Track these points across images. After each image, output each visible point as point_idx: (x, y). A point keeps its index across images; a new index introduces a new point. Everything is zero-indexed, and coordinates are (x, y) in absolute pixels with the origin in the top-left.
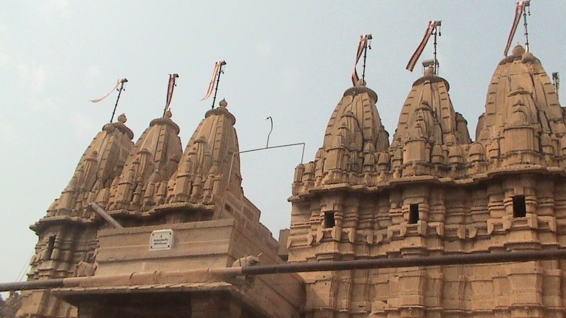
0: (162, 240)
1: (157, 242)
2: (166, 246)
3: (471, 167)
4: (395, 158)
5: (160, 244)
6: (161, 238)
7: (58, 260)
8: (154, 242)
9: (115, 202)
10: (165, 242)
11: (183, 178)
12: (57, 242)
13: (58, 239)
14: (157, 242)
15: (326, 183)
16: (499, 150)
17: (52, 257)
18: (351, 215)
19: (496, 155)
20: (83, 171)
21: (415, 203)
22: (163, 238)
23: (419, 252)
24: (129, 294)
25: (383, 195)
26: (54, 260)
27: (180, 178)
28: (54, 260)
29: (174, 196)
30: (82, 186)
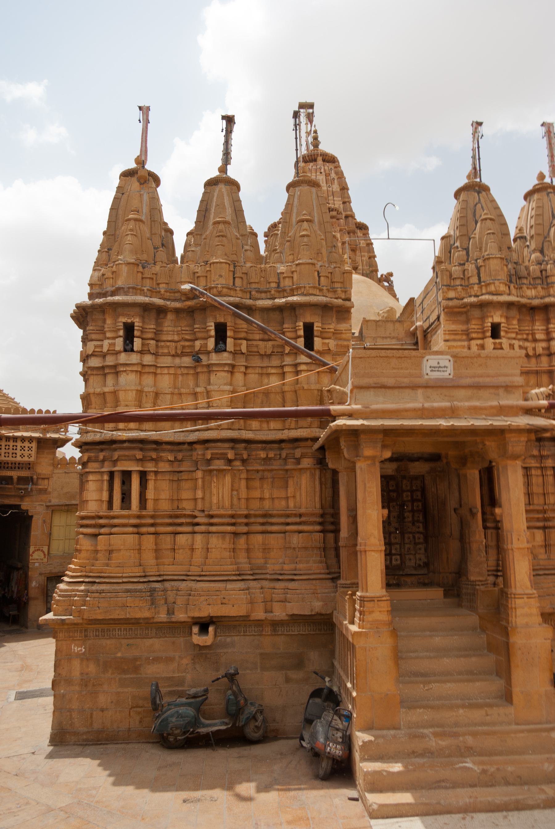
0: (440, 367)
1: (434, 369)
2: (446, 374)
5: (438, 371)
6: (439, 366)
8: (431, 369)
10: (445, 369)
11: (307, 266)
12: (138, 330)
13: (138, 326)
14: (433, 369)
17: (135, 349)
18: (513, 327)
22: (442, 364)
24: (443, 429)
27: (303, 266)
28: (137, 352)
29: (305, 287)
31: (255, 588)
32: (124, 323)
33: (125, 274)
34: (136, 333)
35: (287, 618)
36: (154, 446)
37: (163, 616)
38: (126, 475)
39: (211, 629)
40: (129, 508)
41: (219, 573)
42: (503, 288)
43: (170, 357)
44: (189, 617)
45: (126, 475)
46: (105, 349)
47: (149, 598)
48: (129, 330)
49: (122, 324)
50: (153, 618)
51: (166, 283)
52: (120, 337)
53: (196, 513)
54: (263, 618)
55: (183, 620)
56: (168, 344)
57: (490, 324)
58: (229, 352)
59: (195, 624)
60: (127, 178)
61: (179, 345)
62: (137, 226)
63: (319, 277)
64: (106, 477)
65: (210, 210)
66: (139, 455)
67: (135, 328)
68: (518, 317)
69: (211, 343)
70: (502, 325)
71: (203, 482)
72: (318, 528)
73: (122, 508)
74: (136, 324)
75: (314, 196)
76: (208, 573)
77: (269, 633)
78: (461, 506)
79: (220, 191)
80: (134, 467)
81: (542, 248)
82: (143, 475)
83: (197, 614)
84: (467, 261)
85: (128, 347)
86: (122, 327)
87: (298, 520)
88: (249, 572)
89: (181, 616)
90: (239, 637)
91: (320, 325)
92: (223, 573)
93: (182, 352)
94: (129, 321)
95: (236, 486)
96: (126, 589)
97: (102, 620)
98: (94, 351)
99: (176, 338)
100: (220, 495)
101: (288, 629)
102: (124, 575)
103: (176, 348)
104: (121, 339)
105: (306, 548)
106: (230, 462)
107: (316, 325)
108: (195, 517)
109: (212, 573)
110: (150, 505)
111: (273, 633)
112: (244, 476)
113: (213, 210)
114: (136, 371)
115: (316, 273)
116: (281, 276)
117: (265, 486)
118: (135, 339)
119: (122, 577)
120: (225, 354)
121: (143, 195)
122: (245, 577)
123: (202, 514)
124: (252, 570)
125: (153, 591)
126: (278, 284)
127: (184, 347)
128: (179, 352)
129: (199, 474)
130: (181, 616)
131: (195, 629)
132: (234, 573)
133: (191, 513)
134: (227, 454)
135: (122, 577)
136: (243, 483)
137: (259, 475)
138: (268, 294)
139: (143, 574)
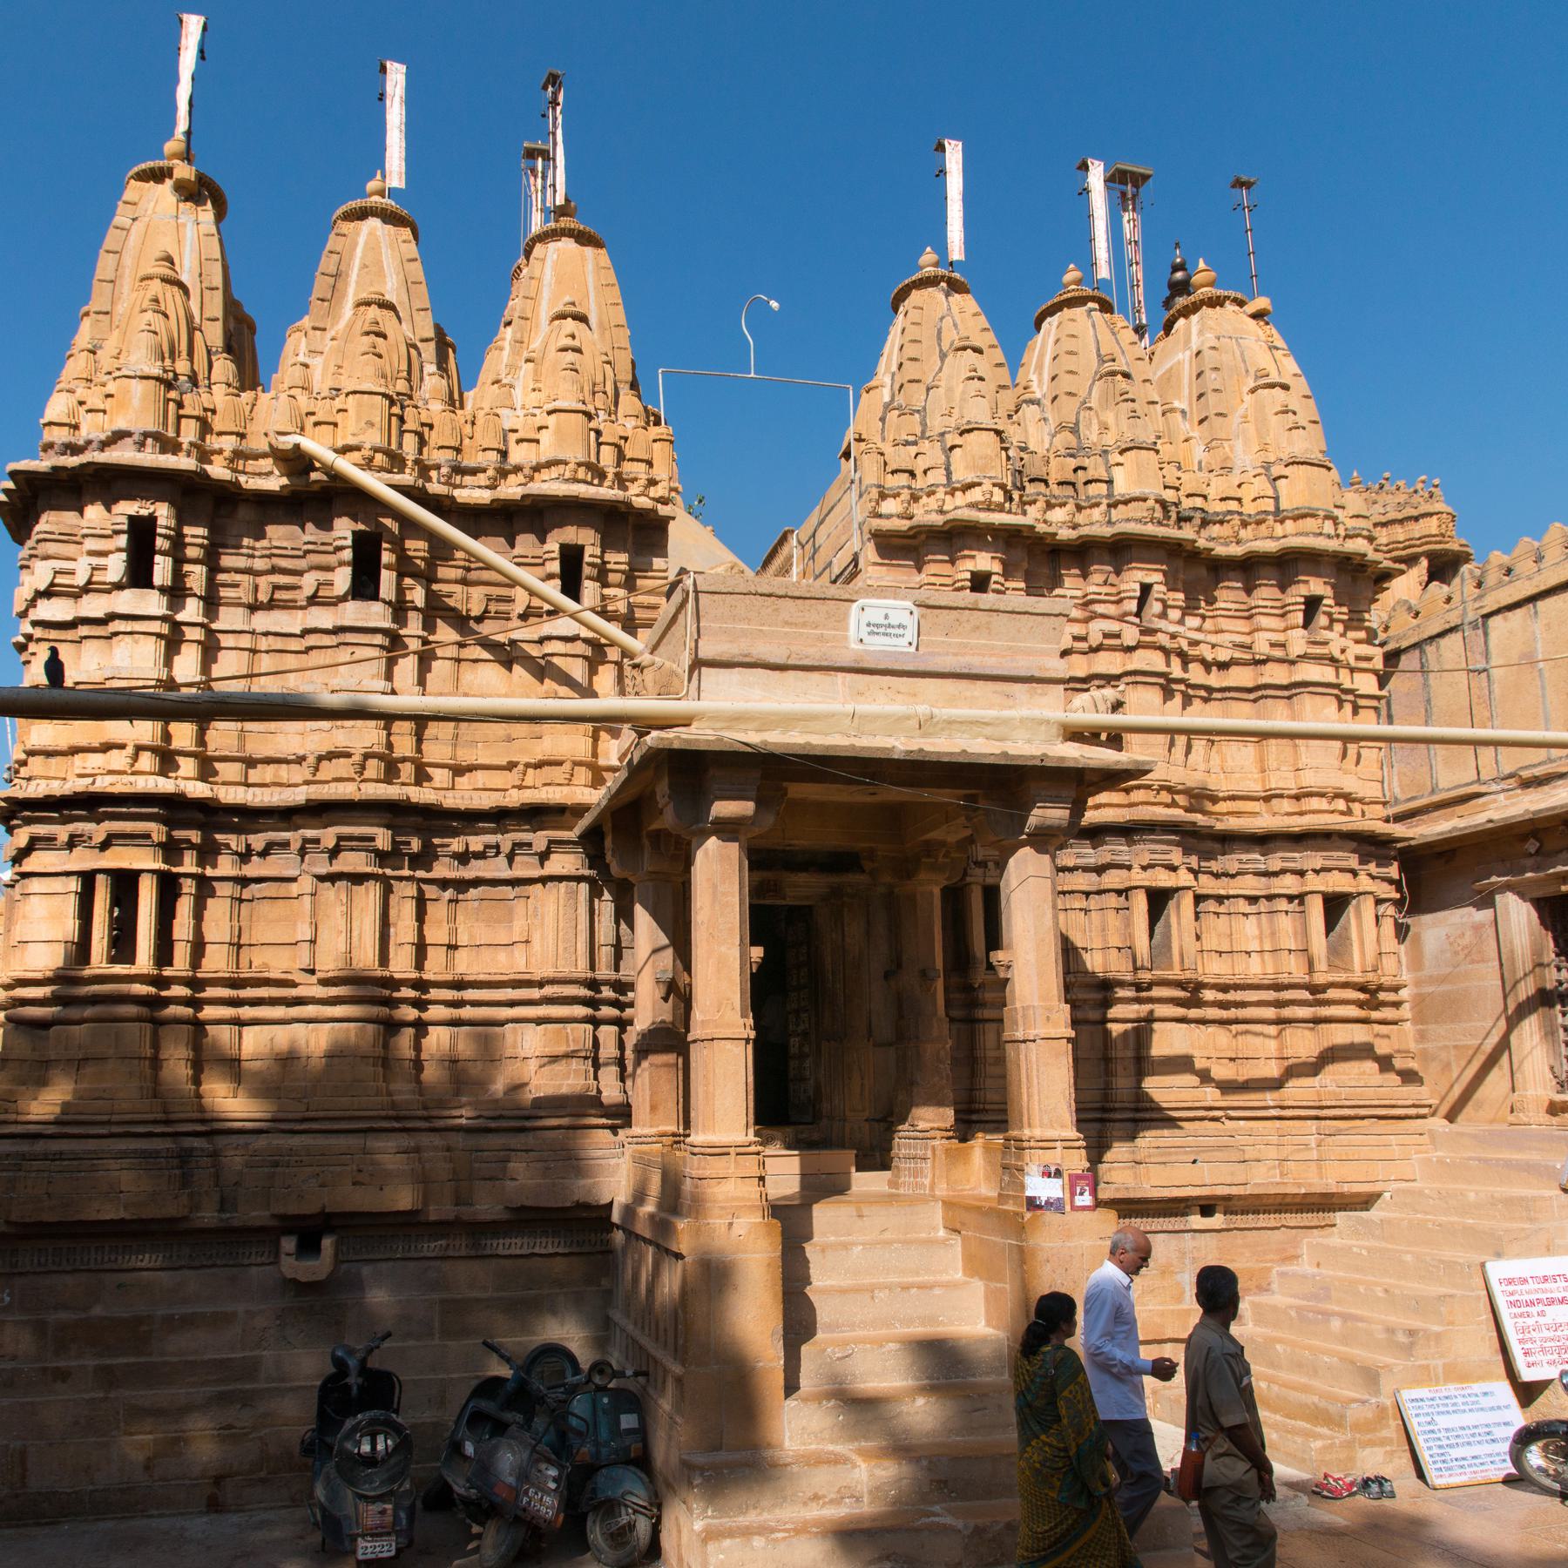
3: (1221, 522)
4: (1091, 474)
7: (176, 593)
9: (368, 446)
12: (165, 536)
15: (972, 505)
16: (1277, 499)
17: (157, 581)
19: (1271, 508)
20: (166, 316)
21: (1148, 580)
23: (1161, 681)
25: (1083, 553)
26: (162, 590)
28: (162, 590)
29: (566, 463)
30: (182, 366)
31: (436, 1148)
32: (131, 518)
33: (136, 402)
34: (161, 543)
35: (505, 1216)
36: (200, 816)
37: (208, 1216)
38: (125, 883)
39: (327, 1243)
40: (131, 960)
41: (348, 1113)
42: (998, 496)
43: (241, 610)
44: (274, 1216)
45: (125, 883)
46: (80, 580)
47: (177, 1172)
48: (141, 534)
49: (125, 520)
50: (185, 1218)
51: (238, 434)
52: (120, 550)
53: (298, 977)
54: (451, 1217)
55: (258, 1223)
56: (238, 577)
57: (968, 576)
58: (384, 602)
59: (288, 1232)
60: (147, 185)
61: (263, 582)
62: (169, 295)
63: (599, 444)
64: (74, 884)
65: (348, 275)
66: (157, 831)
67: (159, 531)
68: (1025, 565)
69: (342, 580)
70: (994, 578)
71: (314, 903)
72: (581, 1011)
73: (113, 960)
74: (161, 521)
75: (590, 267)
76: (321, 1114)
77: (463, 1253)
78: (899, 966)
79: (371, 233)
80: (145, 860)
81: (1077, 423)
82: (168, 887)
83: (293, 1209)
84: (923, 437)
85: (139, 575)
86: (125, 527)
87: (535, 993)
88: (420, 1113)
89: (257, 1215)
90: (391, 1264)
91: (598, 551)
92: (357, 1113)
93: (272, 599)
94: (144, 512)
95: (393, 913)
96: (120, 1151)
97: (60, 1223)
98: (52, 584)
99: (259, 564)
100: (355, 934)
101: (508, 1241)
102: (115, 1118)
103: (256, 588)
104: (124, 556)
105: (554, 1059)
106: (382, 857)
107: (588, 551)
108: (294, 985)
109: (331, 1114)
110: (181, 955)
111: (473, 1253)
112: (410, 890)
113: (354, 277)
114: (159, 636)
115: (593, 434)
116: (513, 437)
117: (460, 918)
118: (158, 558)
119: (109, 1123)
120: (377, 607)
121: (184, 225)
122: (410, 1125)
123: (314, 979)
124: (425, 1108)
125: (184, 1157)
126: (504, 454)
127: (276, 587)
128: (263, 597)
129: (306, 884)
130: (254, 1214)
131: (289, 1244)
132: (383, 1113)
133: (284, 976)
134: (373, 839)
135: (109, 1123)
136: (409, 908)
137: (449, 894)
138: (481, 475)
139: (159, 1116)
